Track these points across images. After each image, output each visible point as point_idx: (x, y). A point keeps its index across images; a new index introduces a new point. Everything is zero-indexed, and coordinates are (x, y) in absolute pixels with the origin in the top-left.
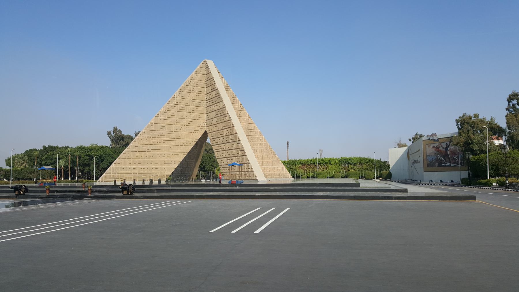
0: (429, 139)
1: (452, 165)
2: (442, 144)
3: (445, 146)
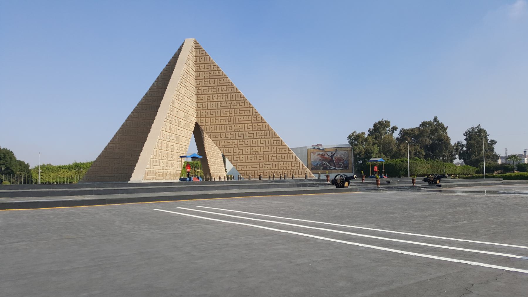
0: (315, 148)
1: (337, 168)
2: (328, 153)
3: (330, 155)
